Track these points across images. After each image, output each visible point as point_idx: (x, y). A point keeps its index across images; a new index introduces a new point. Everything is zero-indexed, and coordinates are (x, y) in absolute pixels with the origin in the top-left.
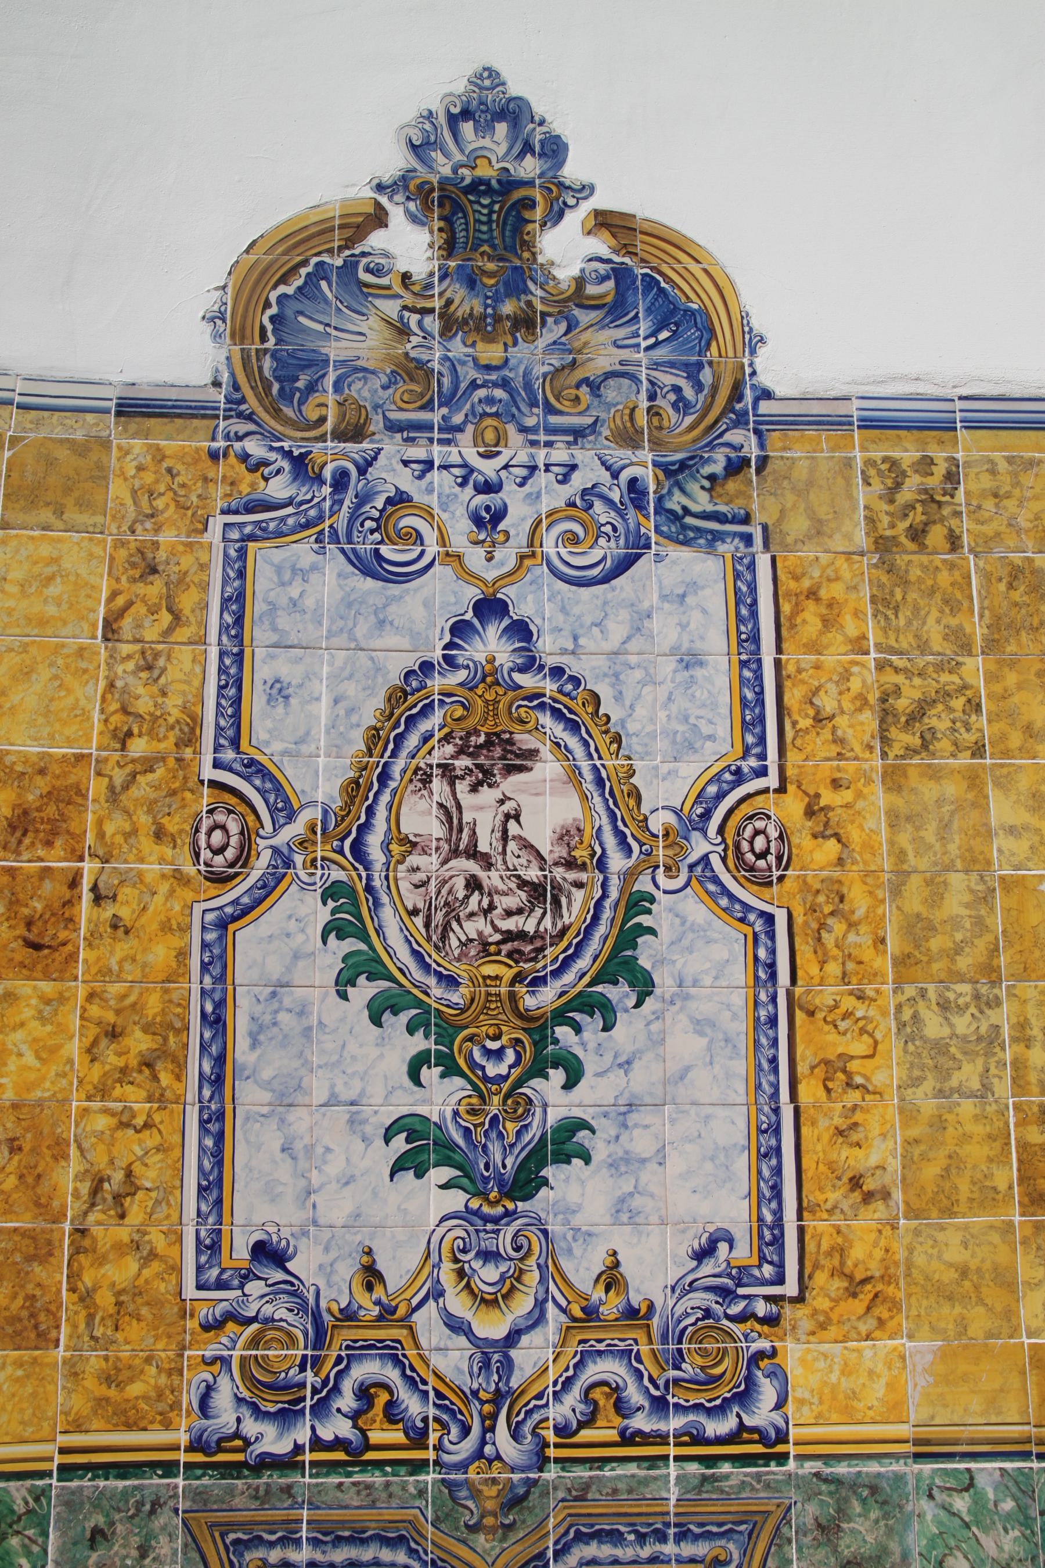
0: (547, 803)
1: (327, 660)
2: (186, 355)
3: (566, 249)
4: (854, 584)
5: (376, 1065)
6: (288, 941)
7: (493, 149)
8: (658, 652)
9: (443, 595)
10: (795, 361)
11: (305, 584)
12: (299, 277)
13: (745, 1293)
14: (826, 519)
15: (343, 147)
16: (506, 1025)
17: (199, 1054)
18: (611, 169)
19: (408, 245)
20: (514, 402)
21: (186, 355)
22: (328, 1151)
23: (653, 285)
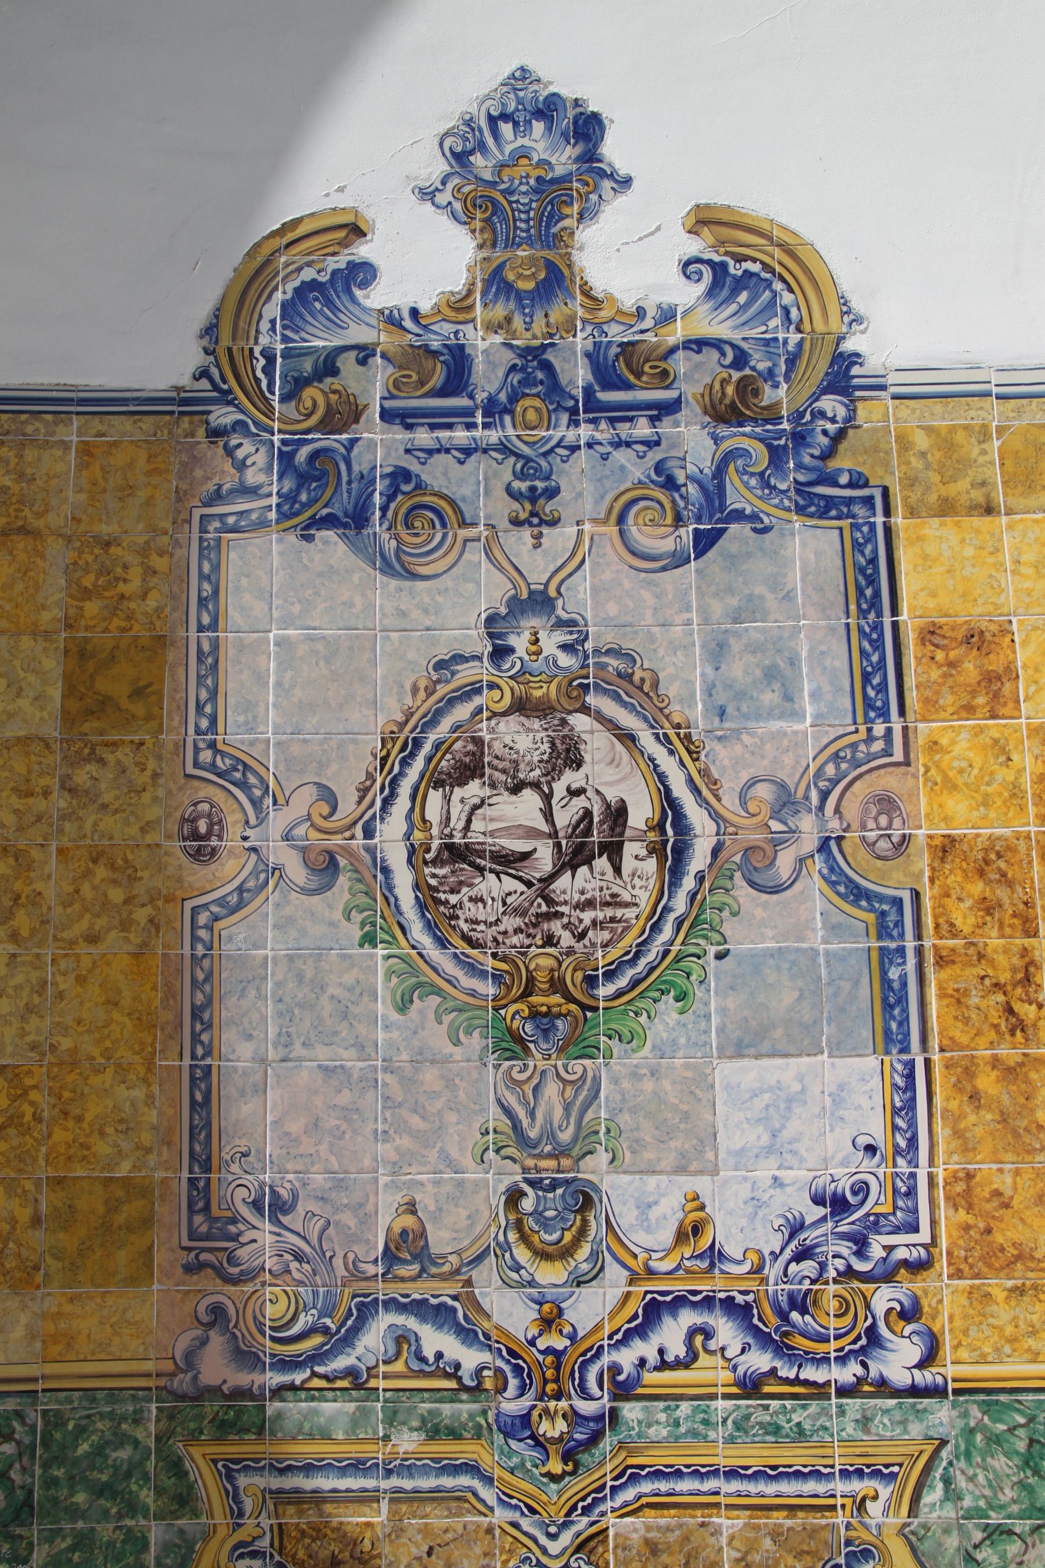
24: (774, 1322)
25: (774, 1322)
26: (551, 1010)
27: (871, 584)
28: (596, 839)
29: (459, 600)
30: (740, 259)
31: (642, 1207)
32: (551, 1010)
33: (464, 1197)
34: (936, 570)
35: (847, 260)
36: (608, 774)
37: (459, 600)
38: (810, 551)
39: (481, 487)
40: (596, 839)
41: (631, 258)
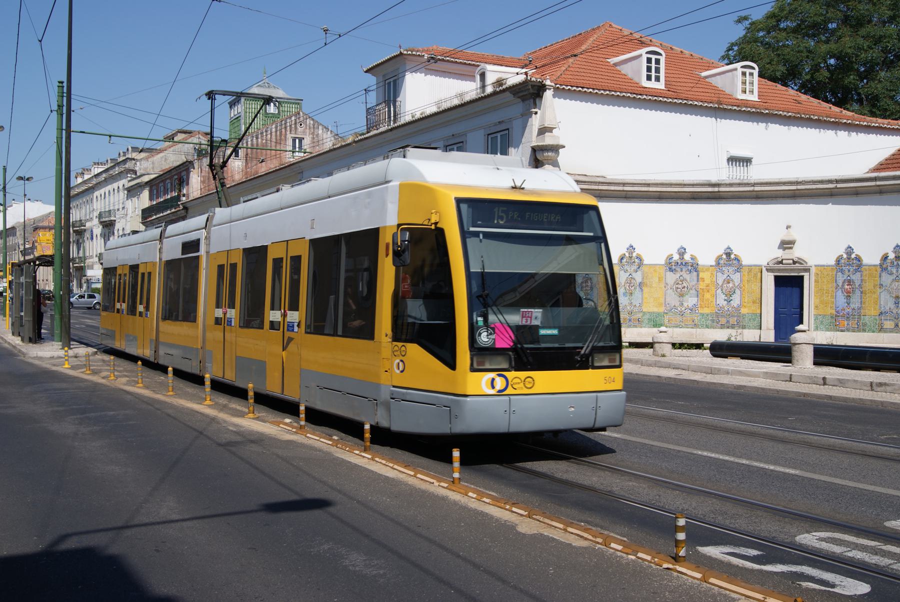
0: (731, 285)
1: (721, 278)
2: (714, 263)
3: (732, 256)
4: (746, 274)
5: (723, 297)
6: (719, 291)
7: (729, 251)
8: (736, 277)
9: (725, 276)
10: (744, 263)
11: (719, 274)
12: (719, 258)
13: (740, 306)
14: (745, 271)
15: (721, 251)
16: (729, 295)
17: (715, 296)
18: (735, 252)
19: (724, 256)
20: (730, 265)
21: (714, 263)
22: (721, 300)
23: (737, 259)
24: (691, 310)
25: (691, 310)
26: (682, 295)
27: (698, 275)
28: (684, 287)
29: (678, 275)
30: (693, 258)
31: (685, 304)
32: (681, 295)
33: (677, 304)
34: (701, 275)
35: (698, 258)
36: (685, 284)
37: (678, 275)
38: (695, 274)
39: (679, 270)
40: (684, 287)
41: (687, 257)
